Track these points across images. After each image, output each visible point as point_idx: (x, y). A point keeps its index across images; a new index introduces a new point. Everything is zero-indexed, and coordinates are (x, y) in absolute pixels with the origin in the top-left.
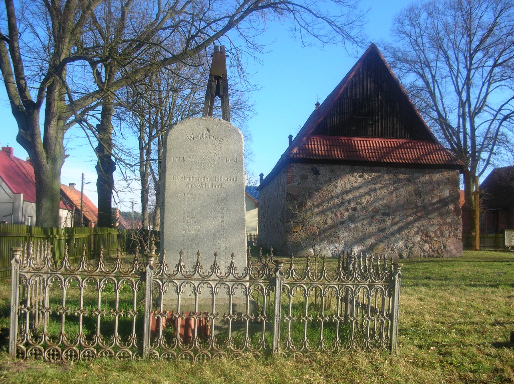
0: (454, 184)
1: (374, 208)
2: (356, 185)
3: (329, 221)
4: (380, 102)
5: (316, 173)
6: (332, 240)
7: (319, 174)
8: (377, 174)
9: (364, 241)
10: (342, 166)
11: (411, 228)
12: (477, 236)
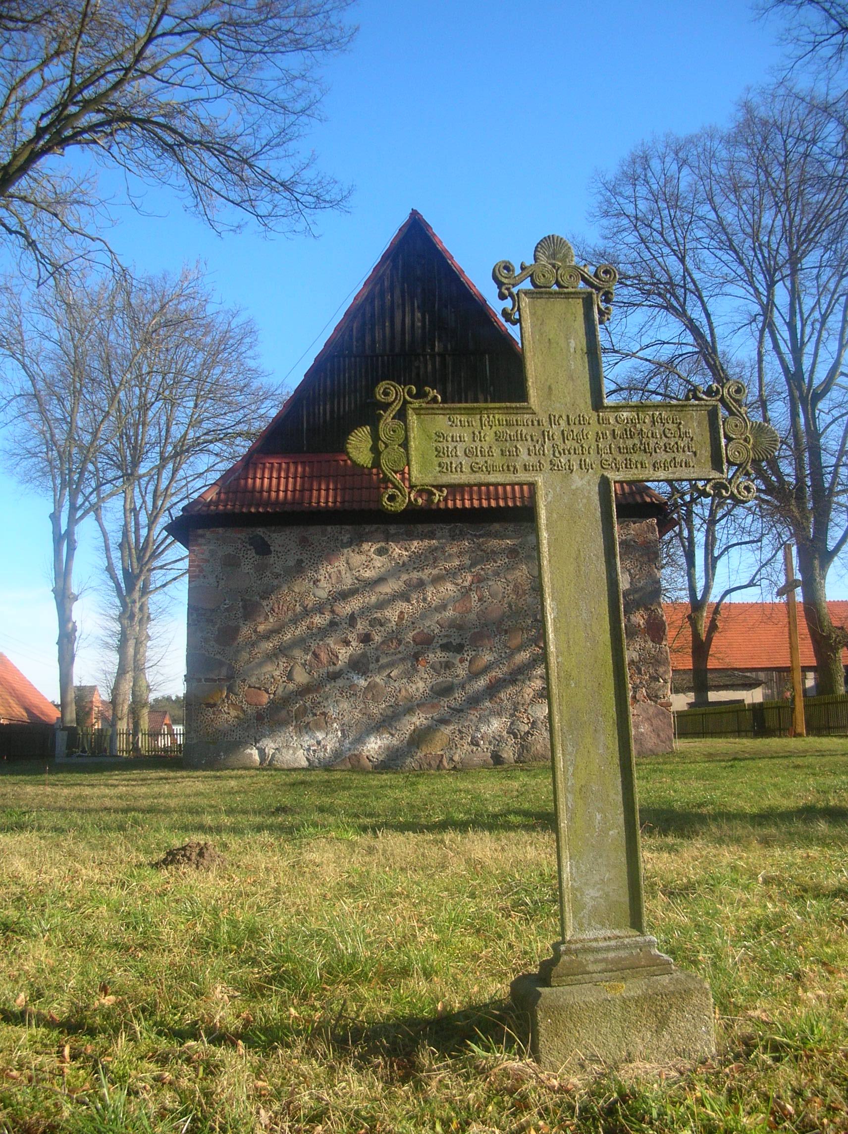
0: (641, 556)
1: (418, 633)
2: (368, 574)
3: (301, 677)
4: (438, 359)
5: (263, 549)
6: (308, 723)
7: (269, 552)
8: (426, 542)
9: (393, 723)
10: (329, 528)
11: (523, 682)
12: (797, 699)
